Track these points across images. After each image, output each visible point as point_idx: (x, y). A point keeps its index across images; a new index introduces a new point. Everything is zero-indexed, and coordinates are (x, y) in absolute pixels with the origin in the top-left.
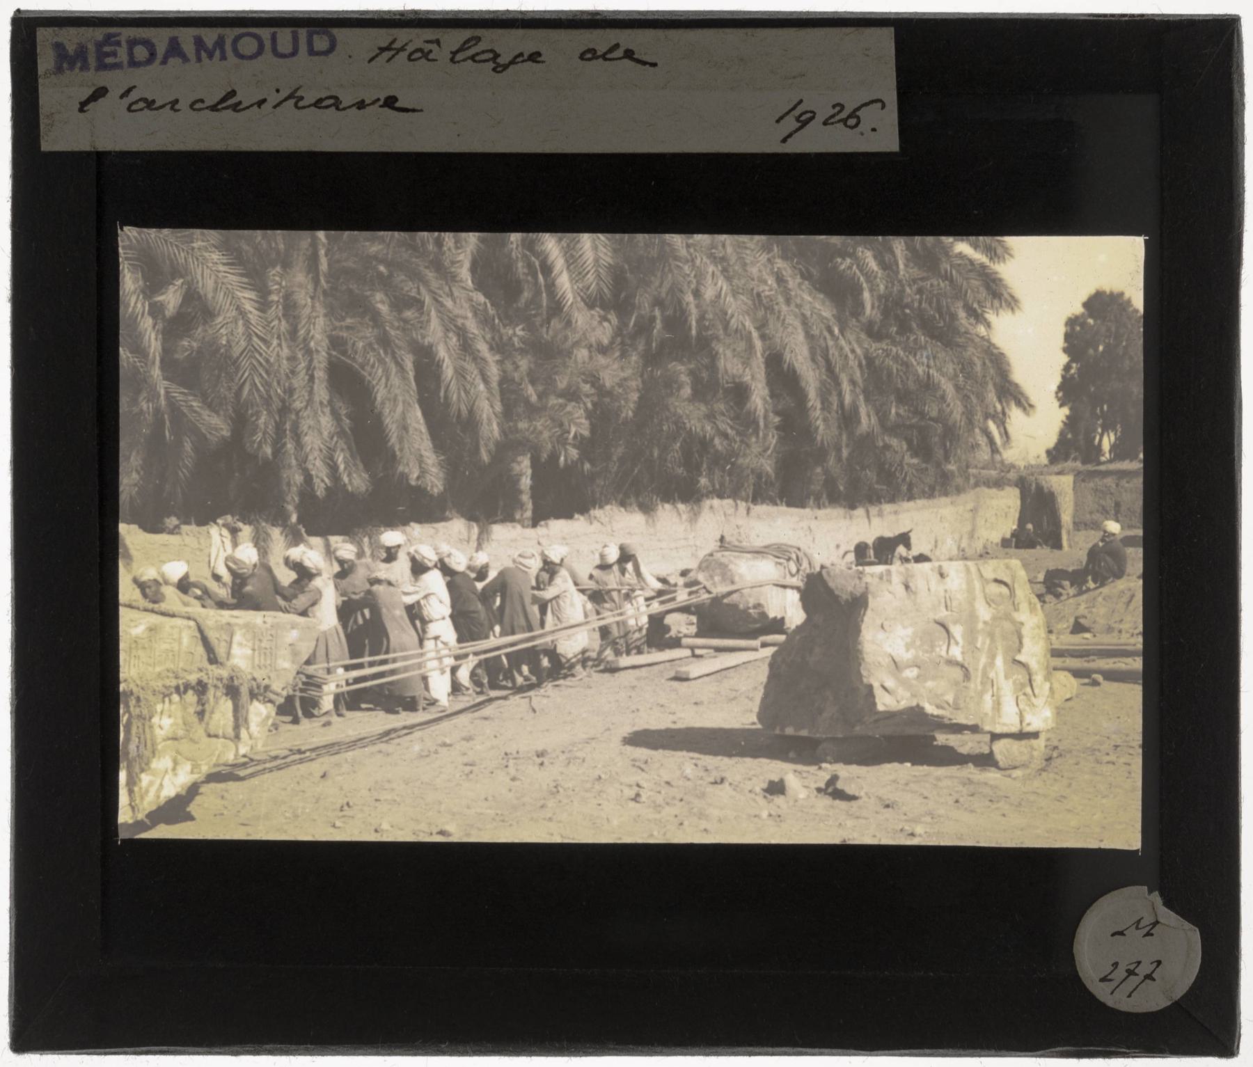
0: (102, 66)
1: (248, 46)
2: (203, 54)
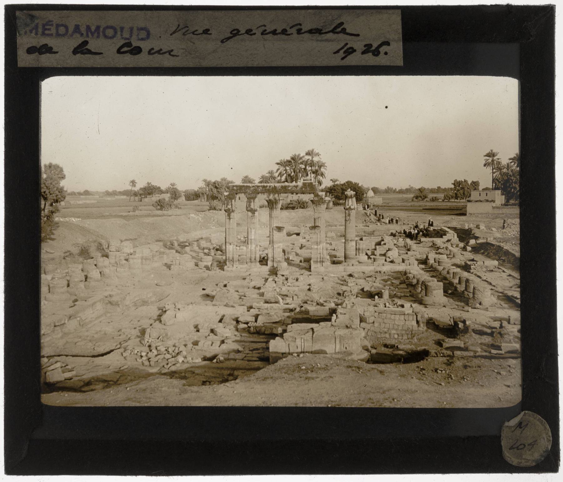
0: (43, 34)
2: (90, 34)
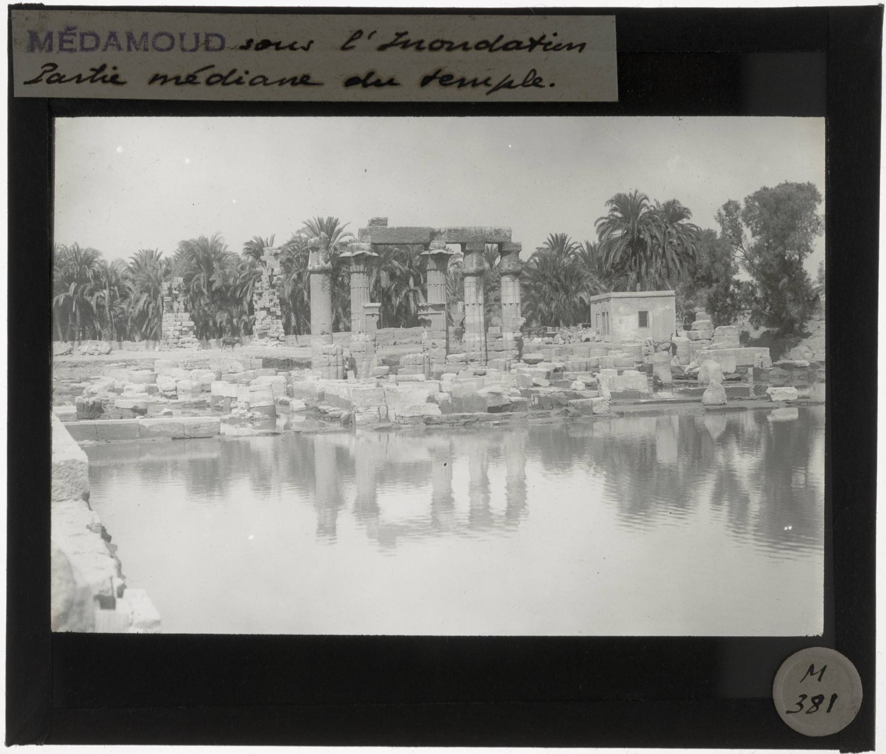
0: (61, 49)
1: (164, 42)
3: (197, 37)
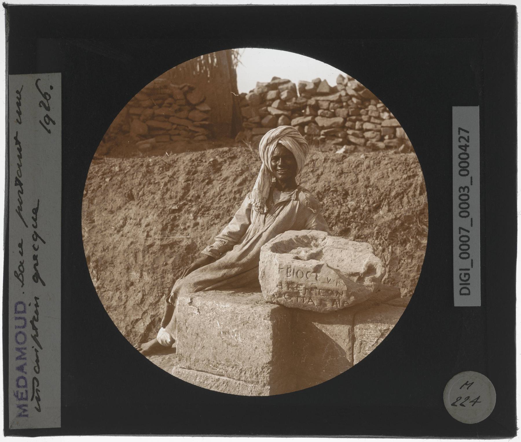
3: (16, 318)
